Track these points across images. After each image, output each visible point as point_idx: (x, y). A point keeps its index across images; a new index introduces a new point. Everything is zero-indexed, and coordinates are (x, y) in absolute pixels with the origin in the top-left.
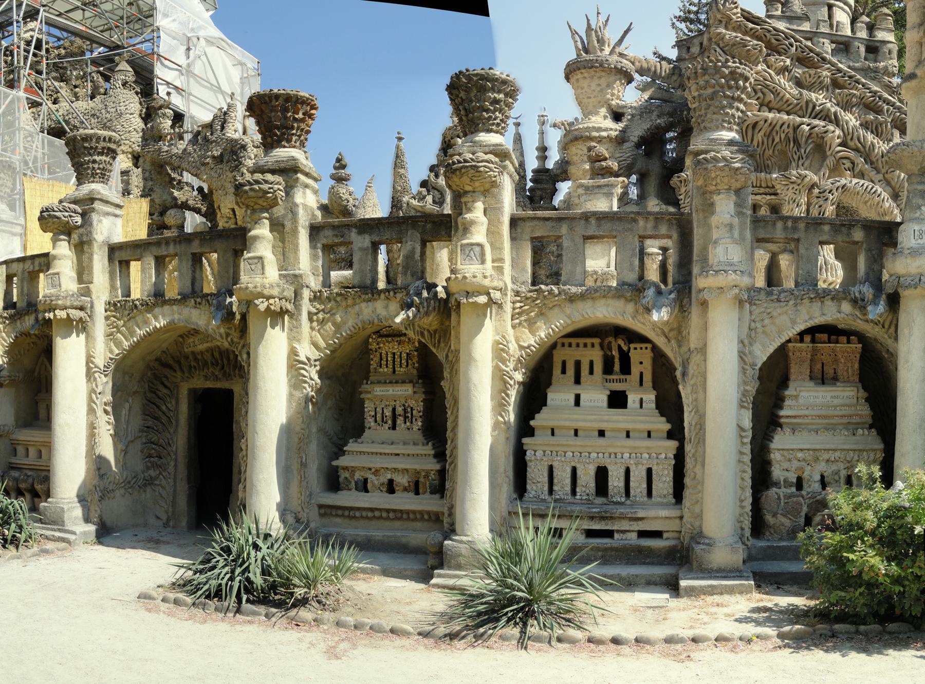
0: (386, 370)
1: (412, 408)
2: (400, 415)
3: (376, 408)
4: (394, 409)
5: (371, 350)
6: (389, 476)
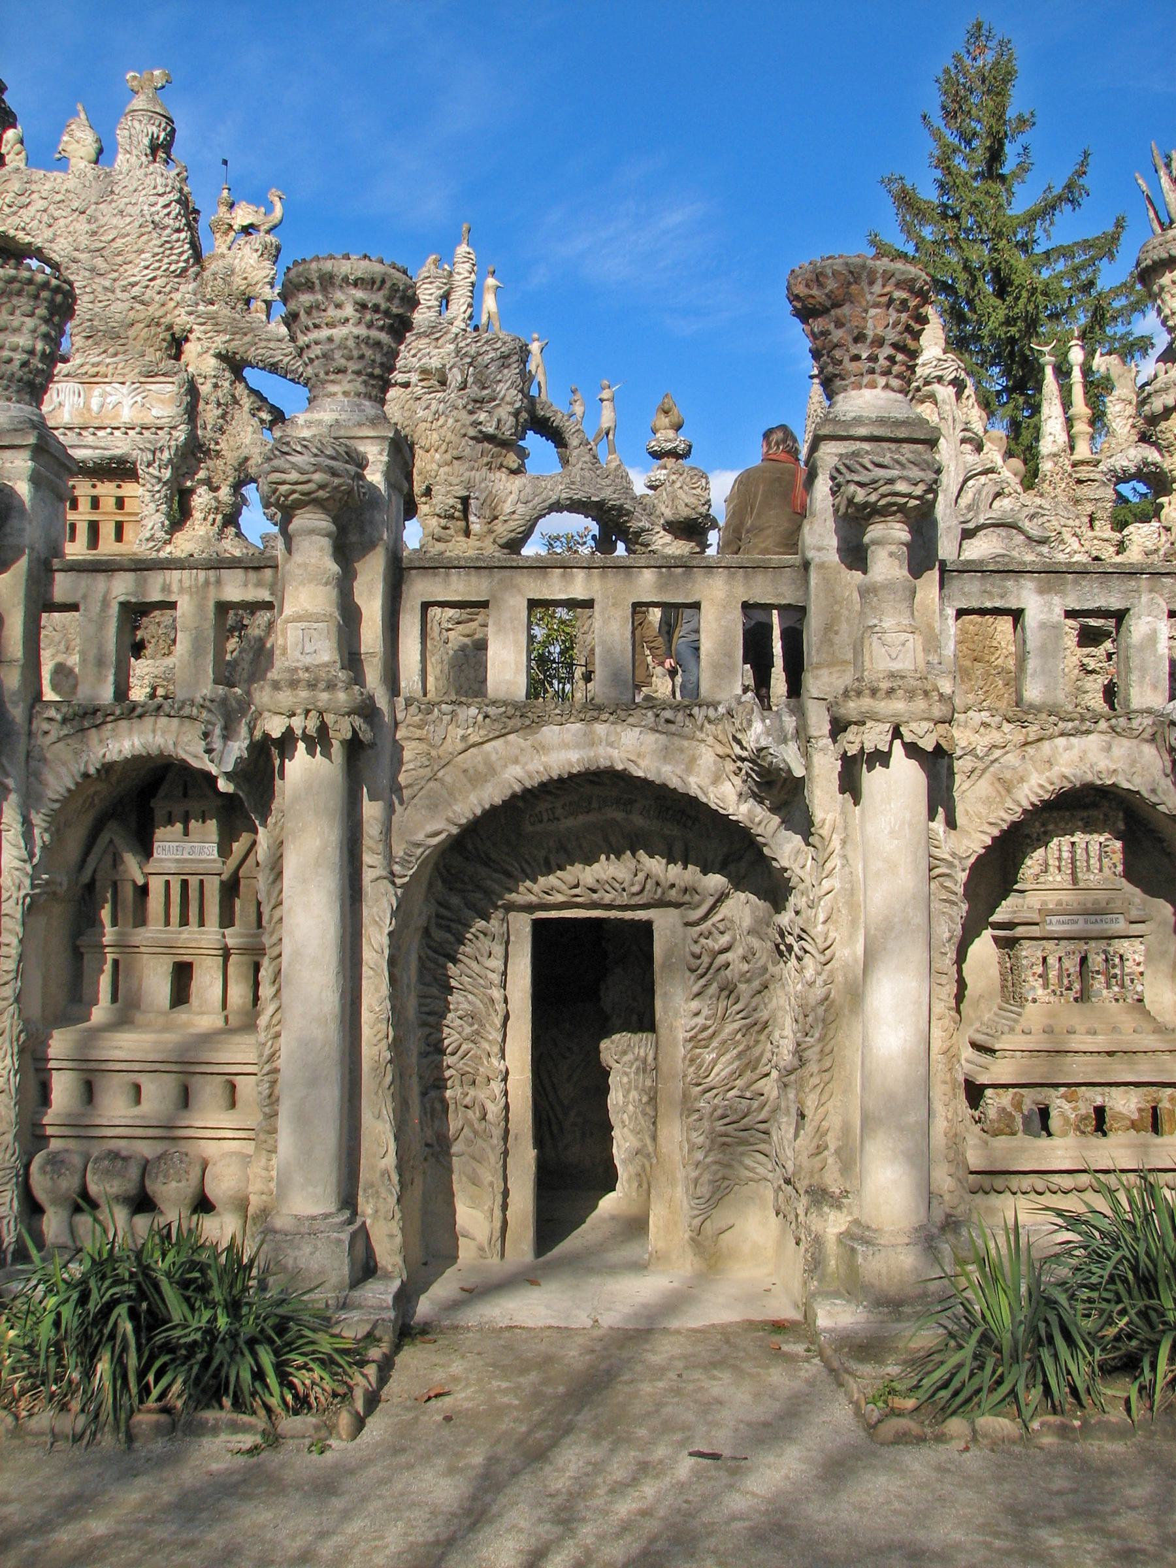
0: (1059, 878)
1: (1121, 957)
2: (1098, 972)
3: (1044, 959)
4: (1084, 960)
5: (1028, 836)
6: (1099, 1101)
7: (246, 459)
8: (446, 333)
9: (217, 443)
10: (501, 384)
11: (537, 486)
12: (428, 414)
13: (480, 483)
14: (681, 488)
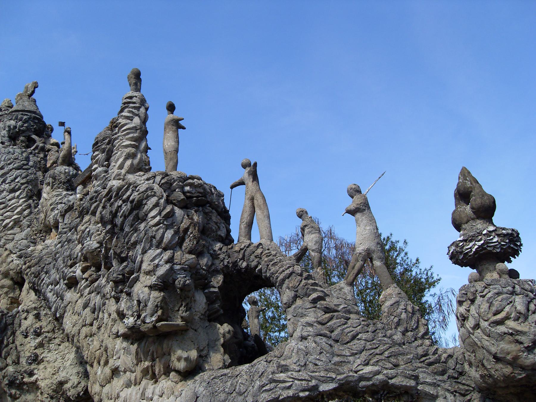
7: (61, 384)
9: (31, 374)
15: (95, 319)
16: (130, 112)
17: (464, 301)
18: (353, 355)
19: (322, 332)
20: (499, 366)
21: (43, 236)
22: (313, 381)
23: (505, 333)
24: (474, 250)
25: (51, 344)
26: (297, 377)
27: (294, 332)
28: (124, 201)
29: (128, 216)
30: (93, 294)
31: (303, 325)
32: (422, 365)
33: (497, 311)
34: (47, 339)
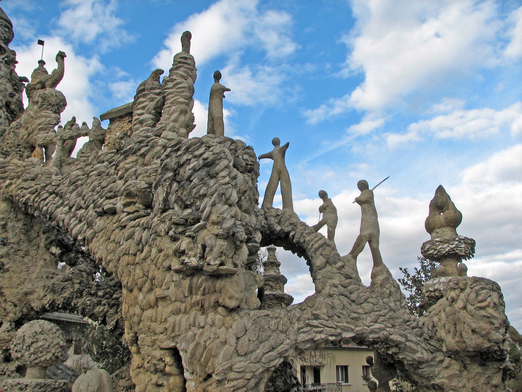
8: (152, 147)
10: (206, 200)
11: (262, 329)
12: (130, 245)
13: (187, 331)
14: (465, 308)
15: (138, 250)
16: (185, 72)
17: (456, 289)
18: (366, 313)
19: (344, 293)
20: (474, 336)
21: (20, 151)
22: (338, 329)
23: (484, 316)
24: (447, 250)
25: (16, 255)
26: (327, 325)
27: (322, 290)
28: (195, 157)
29: (198, 171)
30: (137, 228)
31: (330, 286)
32: (408, 327)
33: (482, 300)
34: (13, 250)
